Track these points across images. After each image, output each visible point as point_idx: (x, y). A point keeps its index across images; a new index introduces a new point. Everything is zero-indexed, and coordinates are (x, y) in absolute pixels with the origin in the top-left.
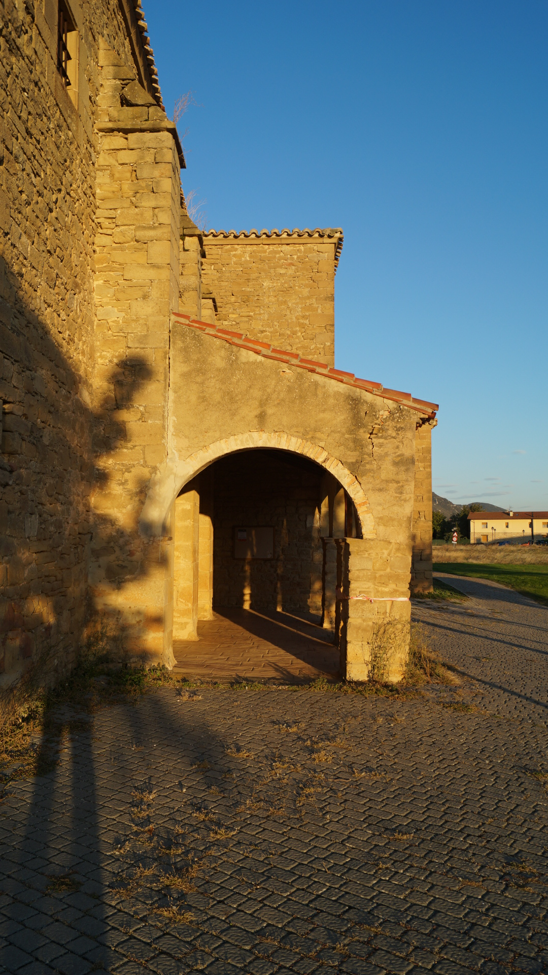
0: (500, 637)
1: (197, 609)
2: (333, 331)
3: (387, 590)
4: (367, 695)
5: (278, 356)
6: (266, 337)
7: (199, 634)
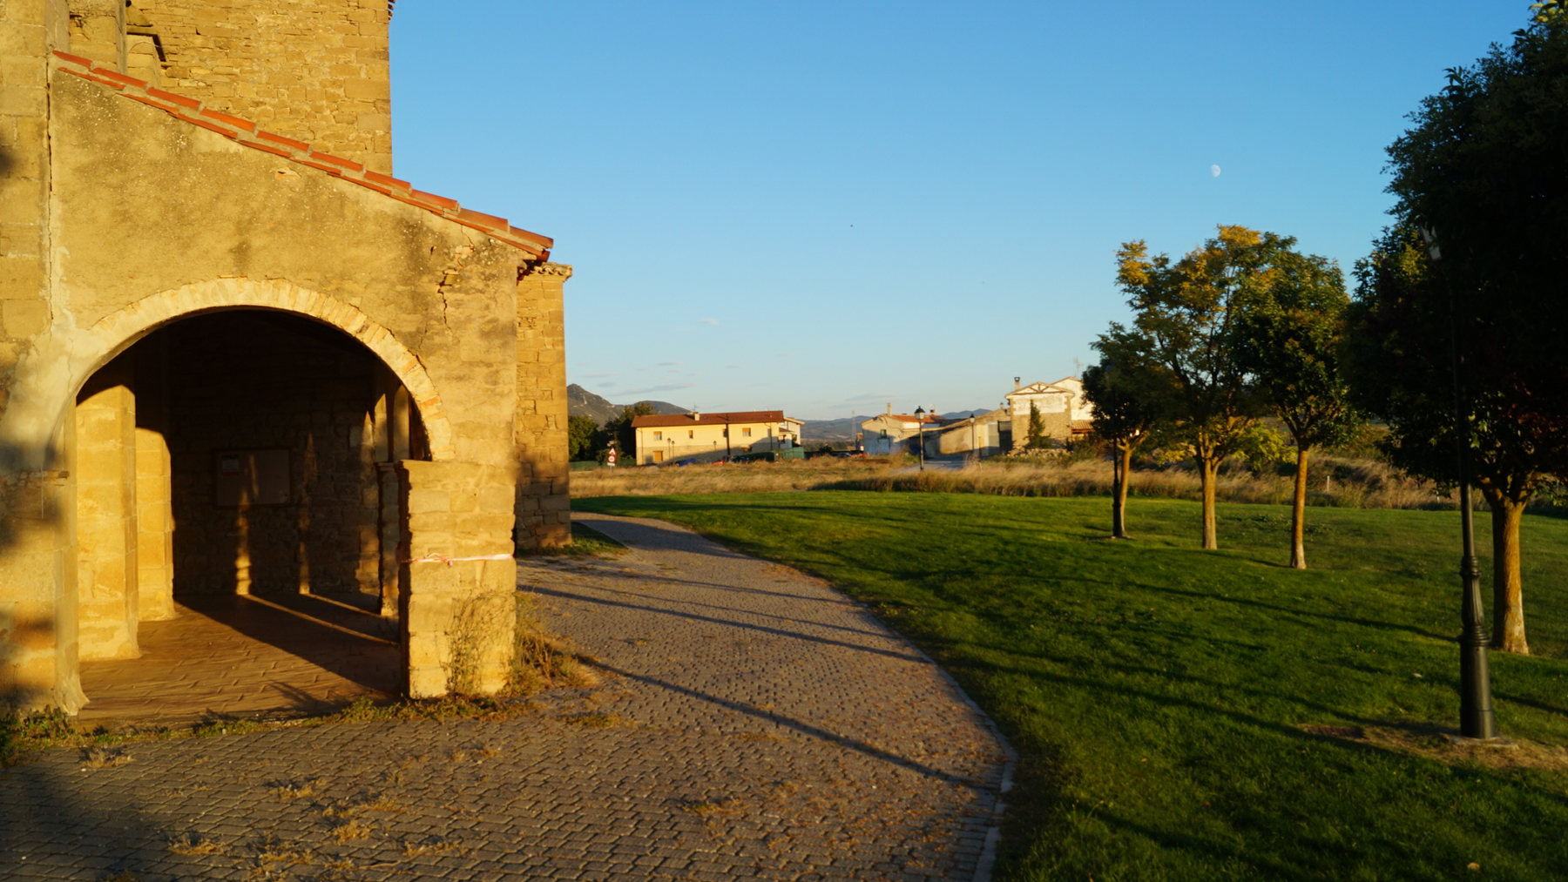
0: (669, 606)
1: (136, 602)
2: (388, 112)
3: (475, 543)
4: (442, 719)
5: (270, 144)
6: (265, 114)
7: (142, 646)
